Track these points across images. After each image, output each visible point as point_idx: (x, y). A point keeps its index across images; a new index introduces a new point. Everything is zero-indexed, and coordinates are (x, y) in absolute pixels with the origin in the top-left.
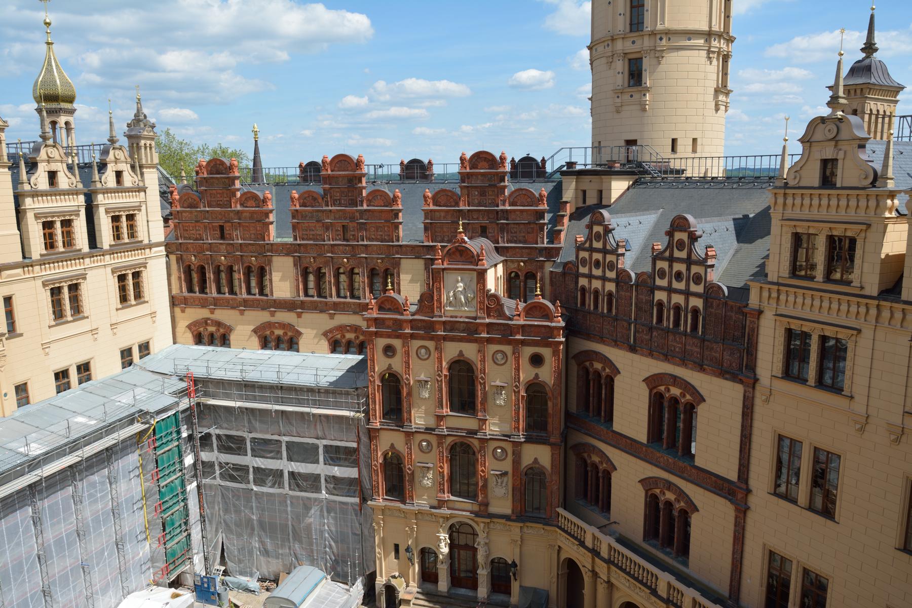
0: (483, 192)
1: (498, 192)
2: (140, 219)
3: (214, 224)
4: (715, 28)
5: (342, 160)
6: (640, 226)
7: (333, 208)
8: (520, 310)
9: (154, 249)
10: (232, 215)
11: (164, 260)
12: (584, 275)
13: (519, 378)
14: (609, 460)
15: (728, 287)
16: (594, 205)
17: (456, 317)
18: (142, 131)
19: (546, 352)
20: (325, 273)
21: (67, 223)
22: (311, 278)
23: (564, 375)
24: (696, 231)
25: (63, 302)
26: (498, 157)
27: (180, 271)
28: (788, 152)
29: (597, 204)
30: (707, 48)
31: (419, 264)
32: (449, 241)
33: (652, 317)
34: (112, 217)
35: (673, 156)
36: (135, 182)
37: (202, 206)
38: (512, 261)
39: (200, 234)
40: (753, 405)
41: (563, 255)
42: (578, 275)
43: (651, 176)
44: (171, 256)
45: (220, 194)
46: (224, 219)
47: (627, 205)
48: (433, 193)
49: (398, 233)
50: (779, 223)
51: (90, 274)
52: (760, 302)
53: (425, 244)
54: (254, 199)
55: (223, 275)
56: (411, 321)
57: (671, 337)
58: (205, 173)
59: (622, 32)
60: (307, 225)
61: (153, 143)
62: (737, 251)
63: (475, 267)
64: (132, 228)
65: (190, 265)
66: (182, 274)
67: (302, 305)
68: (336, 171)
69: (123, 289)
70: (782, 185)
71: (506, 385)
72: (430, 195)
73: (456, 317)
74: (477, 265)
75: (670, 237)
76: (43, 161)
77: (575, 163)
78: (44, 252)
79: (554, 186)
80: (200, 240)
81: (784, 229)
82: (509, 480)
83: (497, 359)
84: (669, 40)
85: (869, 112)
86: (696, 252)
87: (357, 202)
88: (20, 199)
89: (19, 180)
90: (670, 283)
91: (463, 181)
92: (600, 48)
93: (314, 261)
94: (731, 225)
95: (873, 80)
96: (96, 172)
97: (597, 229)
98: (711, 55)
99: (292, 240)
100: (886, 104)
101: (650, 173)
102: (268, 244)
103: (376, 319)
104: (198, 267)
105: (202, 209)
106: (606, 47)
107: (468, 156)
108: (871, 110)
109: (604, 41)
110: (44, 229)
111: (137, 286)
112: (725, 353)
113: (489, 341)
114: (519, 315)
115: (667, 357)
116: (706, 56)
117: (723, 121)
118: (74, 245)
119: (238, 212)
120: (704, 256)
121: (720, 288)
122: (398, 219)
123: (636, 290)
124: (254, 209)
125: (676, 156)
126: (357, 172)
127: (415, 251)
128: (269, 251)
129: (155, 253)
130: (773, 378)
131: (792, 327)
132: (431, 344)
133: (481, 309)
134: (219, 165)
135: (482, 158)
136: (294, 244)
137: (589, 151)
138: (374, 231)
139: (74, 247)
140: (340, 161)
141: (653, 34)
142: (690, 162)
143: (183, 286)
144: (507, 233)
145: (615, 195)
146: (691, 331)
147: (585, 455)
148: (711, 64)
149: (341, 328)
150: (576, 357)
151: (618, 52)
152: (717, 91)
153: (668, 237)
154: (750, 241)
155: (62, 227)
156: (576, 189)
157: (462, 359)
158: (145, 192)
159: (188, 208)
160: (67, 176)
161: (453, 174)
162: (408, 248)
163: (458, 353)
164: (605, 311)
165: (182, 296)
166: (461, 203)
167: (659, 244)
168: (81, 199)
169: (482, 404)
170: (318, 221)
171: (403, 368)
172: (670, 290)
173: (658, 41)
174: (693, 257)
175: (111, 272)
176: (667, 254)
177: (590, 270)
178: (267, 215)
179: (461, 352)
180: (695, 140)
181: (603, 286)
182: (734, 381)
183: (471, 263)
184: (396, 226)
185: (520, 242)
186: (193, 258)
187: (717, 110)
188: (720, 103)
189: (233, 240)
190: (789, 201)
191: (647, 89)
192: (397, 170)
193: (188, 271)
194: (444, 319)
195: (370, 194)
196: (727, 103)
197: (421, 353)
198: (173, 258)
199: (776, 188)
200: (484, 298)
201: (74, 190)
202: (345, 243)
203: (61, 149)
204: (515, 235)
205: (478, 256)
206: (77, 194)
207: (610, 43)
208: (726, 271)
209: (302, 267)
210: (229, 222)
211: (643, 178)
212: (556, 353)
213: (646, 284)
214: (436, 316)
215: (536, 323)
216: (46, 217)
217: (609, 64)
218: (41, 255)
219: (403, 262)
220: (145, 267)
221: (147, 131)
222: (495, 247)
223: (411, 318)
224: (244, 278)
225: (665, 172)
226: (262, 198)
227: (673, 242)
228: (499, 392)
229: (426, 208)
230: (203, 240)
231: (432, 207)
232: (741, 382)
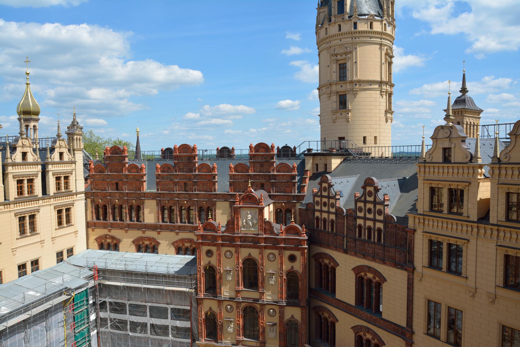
0: (262, 165)
1: (270, 165)
2: (72, 179)
4: (384, 79)
5: (185, 147)
6: (347, 183)
7: (179, 173)
8: (283, 230)
9: (79, 196)
10: (123, 177)
11: (84, 201)
12: (318, 211)
13: (282, 269)
14: (334, 316)
15: (396, 217)
17: (247, 234)
18: (75, 131)
19: (297, 254)
20: (174, 209)
21: (31, 181)
22: (166, 212)
23: (308, 266)
24: (378, 186)
25: (25, 225)
26: (270, 146)
27: (92, 208)
28: (425, 144)
29: (324, 172)
30: (380, 90)
31: (227, 204)
32: (243, 192)
33: (356, 234)
34: (56, 178)
35: (364, 146)
36: (70, 159)
37: (106, 172)
38: (278, 203)
39: (105, 187)
40: (413, 283)
41: (306, 199)
42: (314, 211)
43: (353, 156)
44: (88, 199)
45: (117, 165)
46: (118, 179)
47: (340, 172)
48: (235, 165)
49: (215, 187)
50: (422, 182)
51: (42, 210)
52: (414, 225)
53: (230, 193)
54: (136, 168)
55: (117, 210)
56: (222, 236)
57: (366, 245)
58: (109, 154)
59: (335, 81)
60: (164, 182)
61: (81, 137)
62: (400, 197)
63: (258, 206)
64: (67, 184)
65: (98, 205)
66: (94, 209)
67: (161, 227)
69: (60, 218)
70: (423, 161)
71: (275, 272)
72: (233, 166)
73: (247, 234)
75: (364, 190)
76: (19, 147)
77: (312, 149)
78: (17, 197)
79: (301, 162)
80: (105, 190)
81: (425, 185)
82: (277, 328)
83: (270, 258)
85: (466, 123)
86: (379, 198)
87: (192, 170)
88: (5, 167)
89: (5, 157)
90: (365, 214)
91: (251, 159)
92: (324, 89)
93: (168, 203)
94: (396, 183)
95: (467, 107)
96: (49, 153)
97: (324, 185)
98: (382, 93)
99: (156, 190)
100: (474, 119)
101: (352, 155)
102: (142, 193)
103: (202, 235)
104: (103, 206)
105: (107, 173)
107: (254, 145)
108: (467, 122)
109: (326, 86)
110: (17, 184)
111: (68, 216)
112: (396, 253)
113: (266, 247)
114: (282, 233)
115: (364, 256)
117: (390, 128)
118: (34, 193)
119: (127, 175)
120: (383, 200)
121: (392, 217)
123: (347, 219)
125: (366, 146)
126: (193, 154)
127: (224, 197)
128: (143, 197)
129: (79, 198)
130: (423, 267)
131: (432, 239)
132: (233, 250)
133: (261, 229)
134: (117, 149)
135: (261, 146)
136: (157, 193)
137: (319, 143)
138: (202, 186)
139: (34, 194)
140: (184, 148)
141: (352, 82)
142: (373, 149)
143: (94, 216)
144: (275, 187)
145: (334, 166)
146: (378, 241)
147: (321, 313)
148: (382, 98)
149: (182, 240)
150: (314, 256)
152: (386, 112)
153: (363, 189)
154: (408, 191)
155: (28, 183)
156: (313, 163)
157: (250, 258)
158: (75, 164)
159: (99, 173)
160: (32, 155)
161: (245, 155)
163: (248, 254)
164: (330, 230)
165: (92, 222)
166: (250, 171)
167: (358, 193)
168: (40, 167)
169: (262, 283)
170: (171, 180)
171: (217, 263)
172: (365, 219)
174: (377, 200)
175: (53, 208)
176: (363, 199)
177: (321, 207)
178: (142, 177)
179: (250, 254)
180: (375, 137)
181: (329, 216)
182: (402, 269)
183: (256, 204)
184: (214, 183)
185: (282, 192)
186: (100, 200)
187: (387, 121)
188: (388, 118)
189: (123, 191)
190: (427, 170)
191: (349, 111)
192: (215, 152)
193: (97, 208)
194: (240, 235)
195: (199, 166)
196: (392, 118)
197: (227, 254)
198: (89, 200)
199: (420, 163)
200: (262, 223)
201: (35, 163)
202: (185, 192)
203: (30, 140)
205: (259, 200)
206: (37, 165)
207: (329, 86)
208: (395, 207)
209: (161, 206)
210: (121, 180)
211: (349, 157)
212: (303, 254)
213: (352, 215)
214: (236, 234)
215: (292, 237)
216: (19, 177)
218: (15, 199)
220: (73, 205)
221: (78, 131)
222: (269, 195)
223: (222, 234)
224: (129, 212)
225: (361, 154)
226: (140, 168)
227: (366, 192)
228: (271, 277)
229: (231, 174)
230: (106, 191)
231: (234, 173)
232: (406, 270)
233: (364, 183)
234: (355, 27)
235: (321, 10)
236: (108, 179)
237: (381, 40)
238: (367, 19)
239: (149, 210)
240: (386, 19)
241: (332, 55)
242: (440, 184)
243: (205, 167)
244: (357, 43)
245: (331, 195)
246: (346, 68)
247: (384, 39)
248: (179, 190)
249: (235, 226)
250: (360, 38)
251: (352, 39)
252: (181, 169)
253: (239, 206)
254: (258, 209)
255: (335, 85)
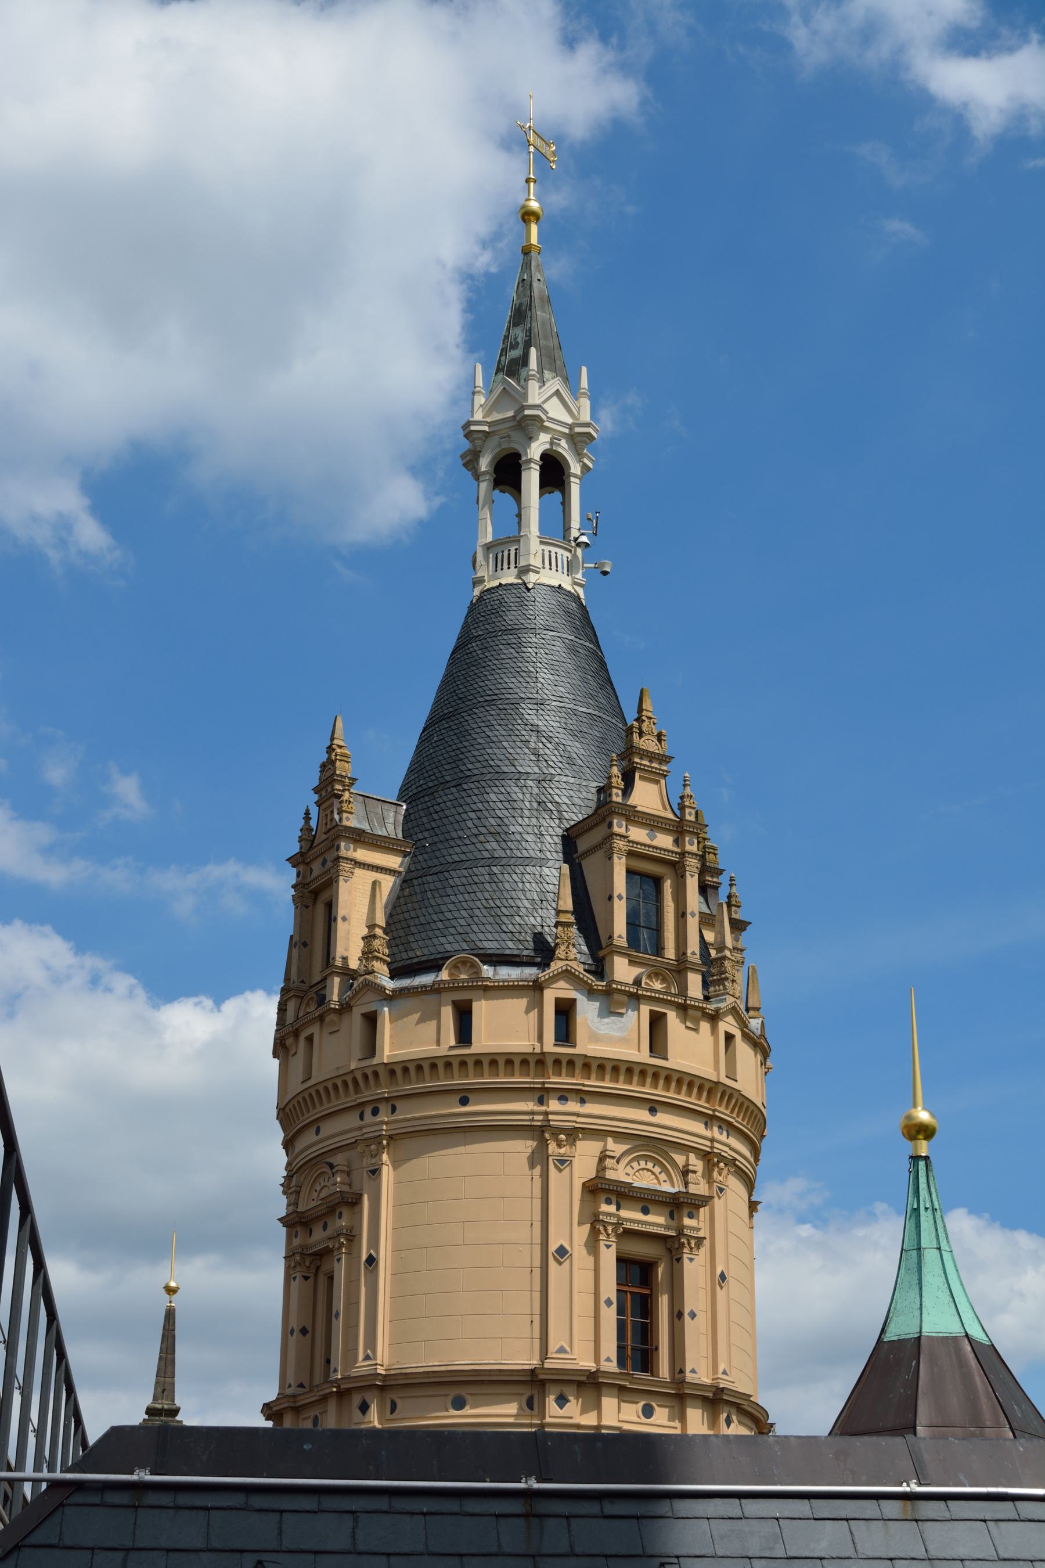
84: (393, 1411)
237: (541, 1101)
238: (436, 989)
240: (567, 974)
247: (563, 1096)
250: (399, 1104)
251: (362, 1117)
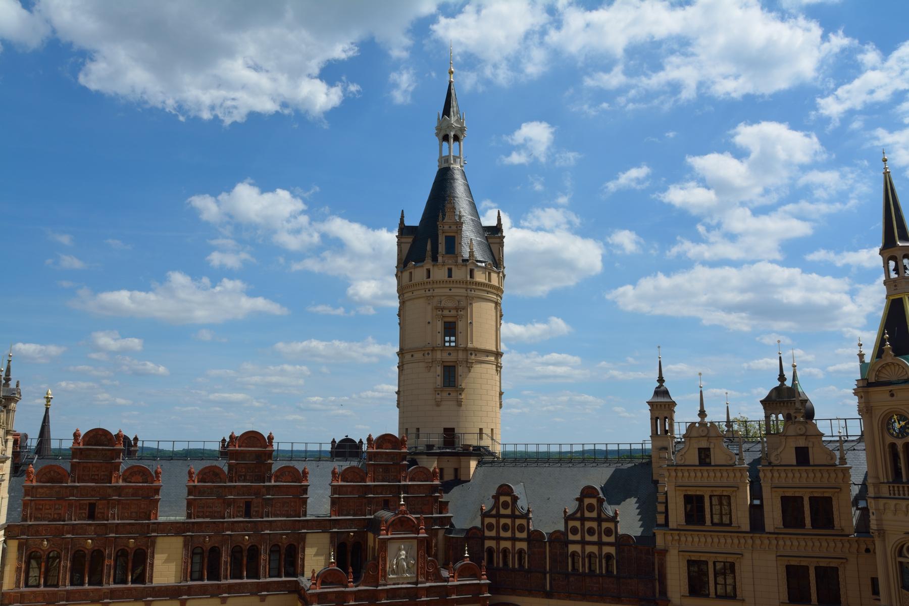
3: (81, 502)
12: (491, 538)
16: (451, 480)
30: (496, 364)
31: (325, 538)
37: (69, 481)
44: (9, 542)
52: (665, 544)
54: (141, 474)
67: (190, 591)
68: (244, 447)
74: (418, 534)
87: (264, 478)
90: (583, 537)
102: (154, 523)
106: (427, 355)
114: (453, 577)
116: (495, 369)
122: (307, 494)
124: (141, 484)
126: (267, 449)
127: (321, 525)
136: (188, 523)
141: (466, 350)
151: (438, 360)
159: (48, 482)
161: (325, 452)
162: (314, 523)
164: (516, 566)
165: (17, 593)
172: (583, 543)
173: (470, 355)
176: (579, 515)
180: (492, 430)
181: (513, 546)
186: (46, 543)
204: (414, 507)
207: (430, 352)
213: (559, 540)
214: (381, 585)
215: (468, 582)
217: (429, 368)
219: (309, 537)
227: (584, 507)
233: (581, 494)
234: (472, 276)
235: (403, 240)
236: (73, 496)
237: (497, 297)
239: (164, 556)
241: (437, 309)
242: (699, 490)
243: (287, 473)
244: (473, 298)
245: (517, 513)
246: (455, 328)
248: (233, 516)
249: (380, 571)
252: (241, 476)
253: (386, 537)
254: (416, 540)
255: (440, 351)
